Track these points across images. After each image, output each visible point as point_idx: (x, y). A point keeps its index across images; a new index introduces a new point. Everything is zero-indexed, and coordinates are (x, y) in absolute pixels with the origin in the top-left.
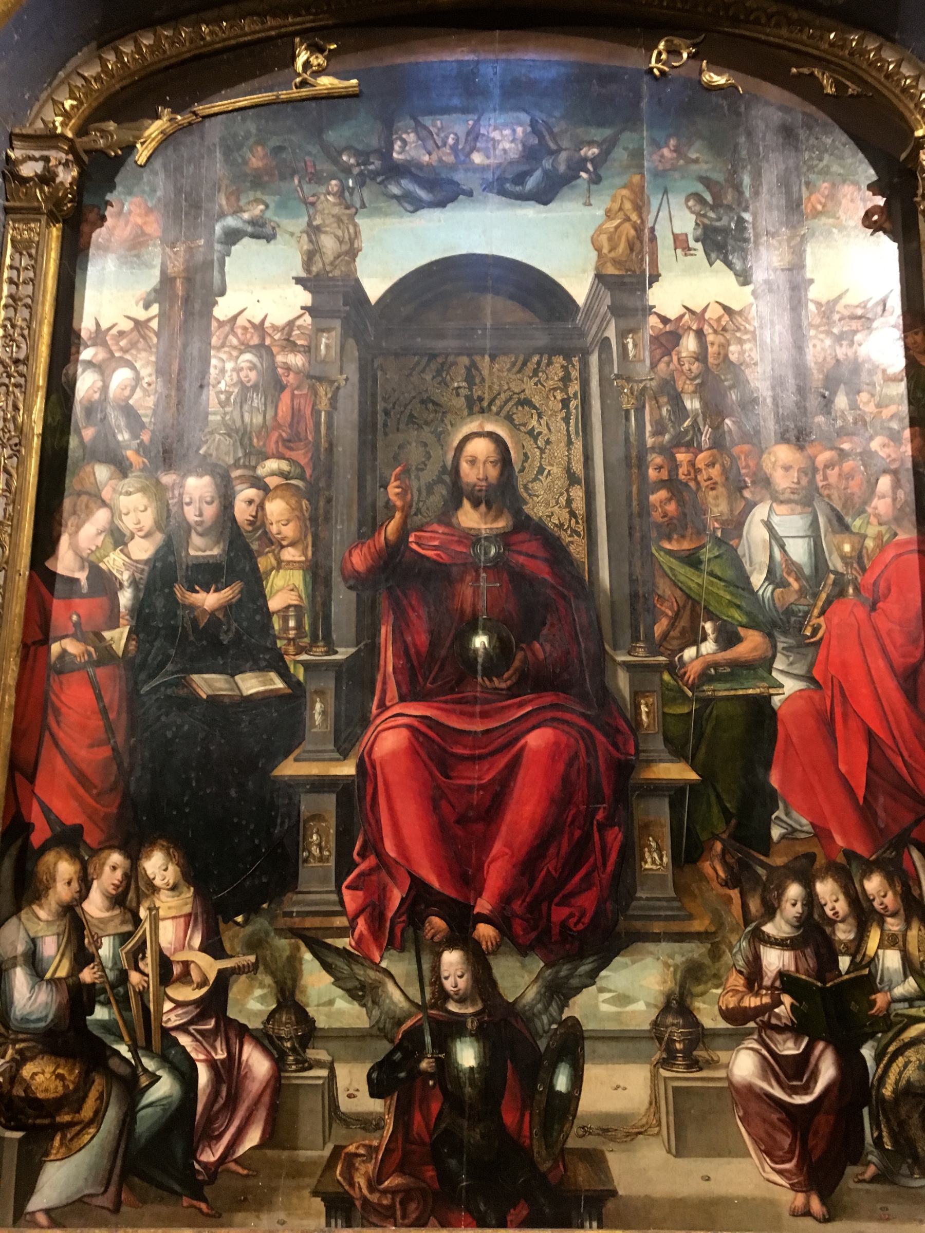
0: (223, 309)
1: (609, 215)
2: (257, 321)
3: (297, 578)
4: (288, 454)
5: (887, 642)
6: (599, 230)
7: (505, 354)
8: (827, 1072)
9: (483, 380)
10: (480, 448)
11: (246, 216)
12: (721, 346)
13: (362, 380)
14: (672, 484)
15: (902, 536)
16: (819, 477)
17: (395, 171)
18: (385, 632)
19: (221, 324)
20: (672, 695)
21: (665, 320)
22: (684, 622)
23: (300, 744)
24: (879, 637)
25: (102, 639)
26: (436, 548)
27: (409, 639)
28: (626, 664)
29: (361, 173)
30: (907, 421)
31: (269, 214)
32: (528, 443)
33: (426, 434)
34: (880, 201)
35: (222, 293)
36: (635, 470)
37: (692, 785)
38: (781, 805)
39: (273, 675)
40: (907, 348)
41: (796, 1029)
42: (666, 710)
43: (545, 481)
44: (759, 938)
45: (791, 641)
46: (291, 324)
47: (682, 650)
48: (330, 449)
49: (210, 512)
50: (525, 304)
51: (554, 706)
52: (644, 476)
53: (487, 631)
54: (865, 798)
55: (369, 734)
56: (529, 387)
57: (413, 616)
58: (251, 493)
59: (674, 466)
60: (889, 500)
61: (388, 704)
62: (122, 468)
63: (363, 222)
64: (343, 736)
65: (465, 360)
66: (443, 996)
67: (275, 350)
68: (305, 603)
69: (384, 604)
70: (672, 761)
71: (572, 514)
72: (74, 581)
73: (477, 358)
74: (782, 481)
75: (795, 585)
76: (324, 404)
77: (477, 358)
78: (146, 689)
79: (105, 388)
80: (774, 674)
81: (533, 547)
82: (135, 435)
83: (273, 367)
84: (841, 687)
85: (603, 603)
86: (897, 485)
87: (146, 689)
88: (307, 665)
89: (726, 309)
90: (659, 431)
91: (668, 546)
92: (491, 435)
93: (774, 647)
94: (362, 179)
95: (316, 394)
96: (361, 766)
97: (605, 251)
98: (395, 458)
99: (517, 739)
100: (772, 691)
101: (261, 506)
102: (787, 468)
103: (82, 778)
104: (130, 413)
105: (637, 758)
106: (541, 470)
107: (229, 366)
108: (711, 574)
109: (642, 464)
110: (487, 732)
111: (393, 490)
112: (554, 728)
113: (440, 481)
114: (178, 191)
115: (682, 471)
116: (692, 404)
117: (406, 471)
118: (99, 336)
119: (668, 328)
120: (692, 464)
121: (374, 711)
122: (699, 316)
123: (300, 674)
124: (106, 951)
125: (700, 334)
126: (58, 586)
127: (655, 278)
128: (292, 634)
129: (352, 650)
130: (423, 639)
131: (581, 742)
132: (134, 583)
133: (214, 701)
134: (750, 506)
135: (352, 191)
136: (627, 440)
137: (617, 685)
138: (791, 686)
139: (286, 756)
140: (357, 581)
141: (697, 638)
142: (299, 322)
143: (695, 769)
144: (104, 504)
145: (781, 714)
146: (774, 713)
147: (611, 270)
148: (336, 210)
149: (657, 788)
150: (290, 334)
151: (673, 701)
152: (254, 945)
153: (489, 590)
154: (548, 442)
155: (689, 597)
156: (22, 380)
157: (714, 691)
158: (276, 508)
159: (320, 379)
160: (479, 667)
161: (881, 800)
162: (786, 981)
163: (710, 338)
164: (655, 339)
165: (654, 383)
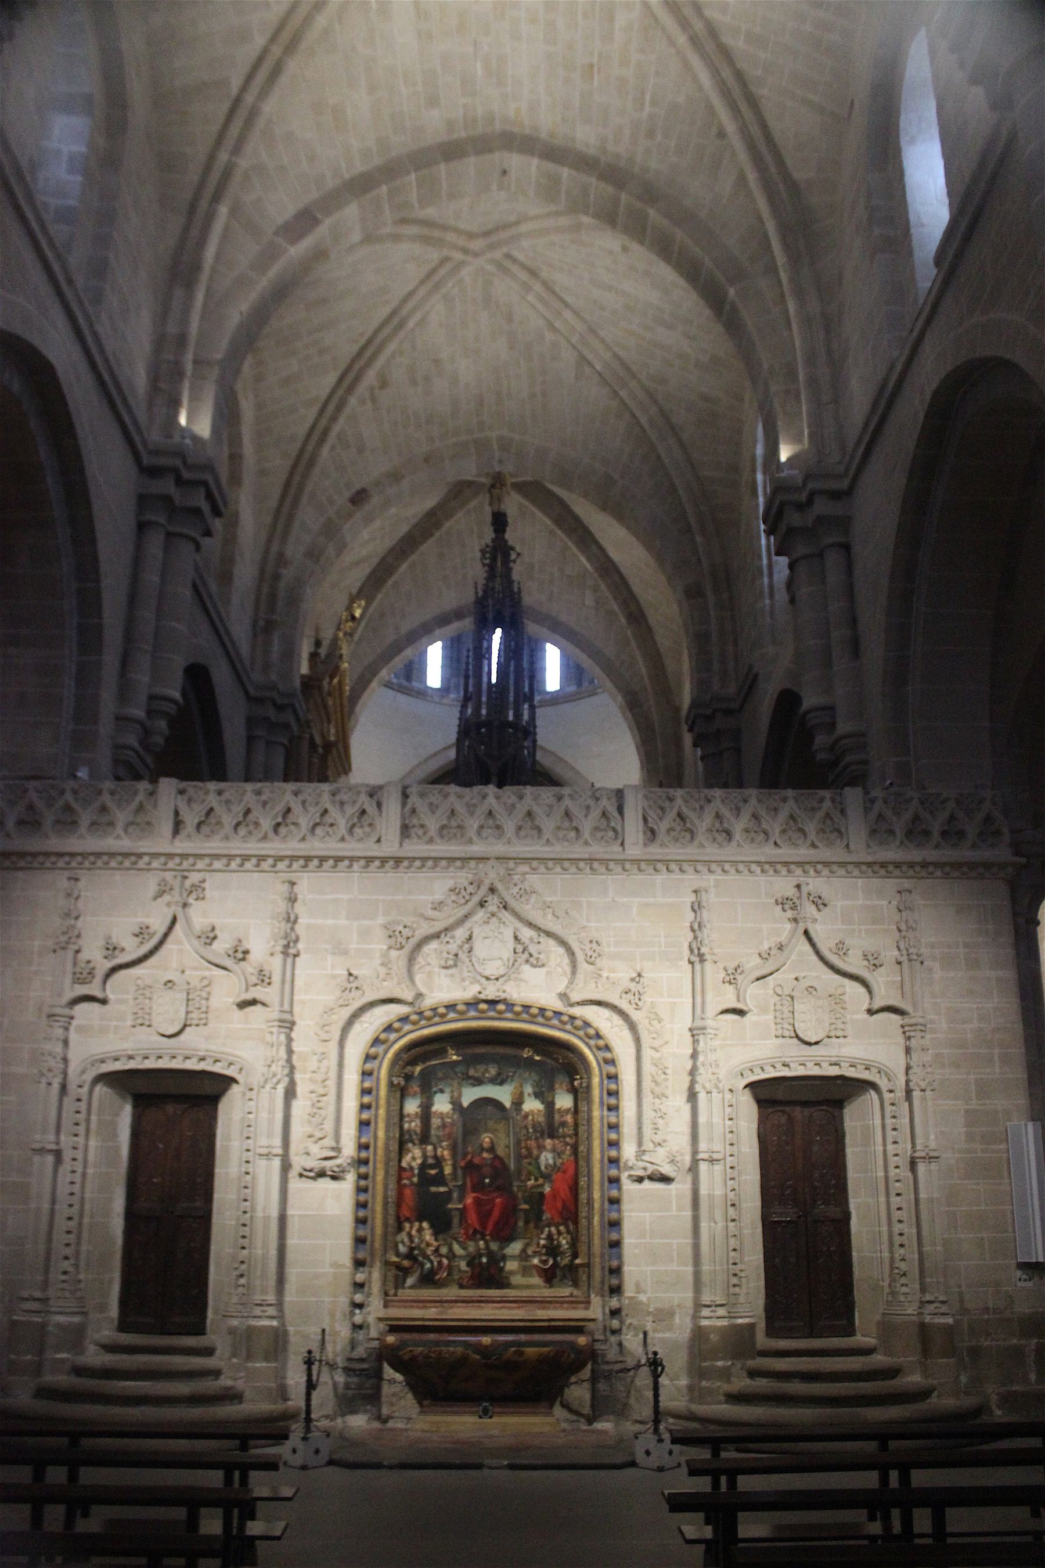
0: (434, 1109)
8: (551, 1262)
10: (487, 1140)
17: (470, 1077)
41: (546, 1254)
44: (540, 1238)
62: (414, 1144)
66: (479, 1249)
74: (549, 1147)
104: (415, 1131)
116: (531, 1130)
118: (409, 1115)
124: (416, 1240)
141: (530, 1180)
149: (522, 1210)
152: (444, 1240)
162: (544, 1246)
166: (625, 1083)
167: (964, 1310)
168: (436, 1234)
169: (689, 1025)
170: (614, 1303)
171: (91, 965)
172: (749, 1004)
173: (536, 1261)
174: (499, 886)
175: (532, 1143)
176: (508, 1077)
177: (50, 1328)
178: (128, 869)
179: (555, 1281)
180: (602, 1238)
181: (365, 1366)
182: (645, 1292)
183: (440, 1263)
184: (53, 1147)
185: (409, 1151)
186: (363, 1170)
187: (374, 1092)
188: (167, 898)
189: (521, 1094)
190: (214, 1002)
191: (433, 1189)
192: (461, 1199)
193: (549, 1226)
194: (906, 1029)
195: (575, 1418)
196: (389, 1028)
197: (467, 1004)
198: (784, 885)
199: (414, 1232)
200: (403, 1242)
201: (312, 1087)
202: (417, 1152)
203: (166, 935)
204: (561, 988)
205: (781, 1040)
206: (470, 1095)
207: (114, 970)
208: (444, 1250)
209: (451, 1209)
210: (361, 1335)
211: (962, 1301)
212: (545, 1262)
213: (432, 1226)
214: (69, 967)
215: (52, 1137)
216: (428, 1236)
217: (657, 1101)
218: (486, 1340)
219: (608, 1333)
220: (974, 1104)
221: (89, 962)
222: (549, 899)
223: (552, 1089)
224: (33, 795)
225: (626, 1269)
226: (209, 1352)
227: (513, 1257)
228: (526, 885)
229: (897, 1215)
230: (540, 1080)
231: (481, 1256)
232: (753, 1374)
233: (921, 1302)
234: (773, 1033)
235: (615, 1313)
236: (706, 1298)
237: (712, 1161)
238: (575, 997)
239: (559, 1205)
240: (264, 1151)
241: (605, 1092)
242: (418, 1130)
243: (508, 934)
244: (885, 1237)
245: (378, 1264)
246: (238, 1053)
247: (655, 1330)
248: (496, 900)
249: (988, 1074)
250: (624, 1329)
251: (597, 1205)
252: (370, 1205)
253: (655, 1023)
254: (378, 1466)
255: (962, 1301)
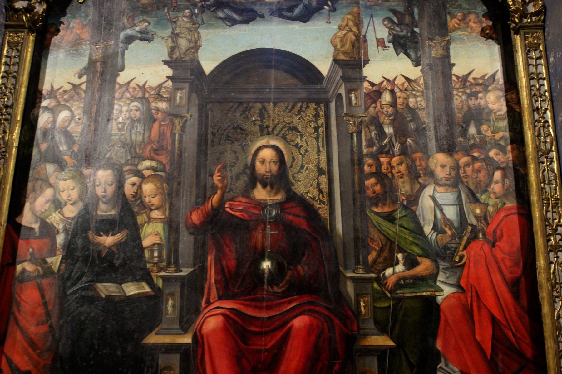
0: (122, 78)
1: (340, 28)
2: (141, 84)
3: (159, 228)
4: (156, 157)
5: (502, 265)
6: (335, 36)
7: (282, 102)
9: (269, 116)
10: (267, 154)
11: (137, 29)
12: (404, 98)
13: (200, 116)
14: (378, 175)
15: (509, 205)
16: (461, 171)
18: (211, 259)
19: (121, 86)
20: (379, 296)
21: (372, 84)
22: (385, 254)
23: (159, 324)
24: (497, 262)
25: (46, 262)
26: (240, 211)
27: (224, 263)
28: (351, 278)
29: (202, 6)
30: (509, 141)
31: (150, 28)
32: (295, 152)
33: (236, 146)
34: (490, 23)
35: (122, 69)
36: (357, 167)
37: (390, 348)
38: (443, 360)
39: (144, 284)
40: (507, 101)
42: (376, 305)
43: (305, 173)
45: (447, 264)
46: (160, 86)
47: (384, 270)
48: (180, 155)
49: (110, 190)
50: (294, 75)
51: (309, 303)
52: (362, 170)
53: (271, 259)
54: (491, 355)
55: (200, 319)
56: (296, 120)
57: (227, 250)
58: (134, 179)
59: (379, 165)
60: (500, 185)
61: (212, 301)
62: (61, 165)
63: (203, 31)
64: (185, 320)
65: (259, 105)
67: (151, 100)
68: (164, 242)
69: (210, 243)
70: (379, 335)
71: (320, 191)
72: (31, 229)
73: (266, 104)
74: (441, 173)
75: (449, 233)
76: (178, 129)
77: (266, 104)
78: (70, 291)
79: (54, 122)
80: (438, 283)
81: (298, 210)
82: (70, 148)
83: (149, 109)
84: (476, 291)
85: (338, 242)
86: (504, 176)
87: (70, 291)
88: (164, 278)
89: (407, 79)
90: (370, 144)
91: (376, 210)
92: (274, 147)
93: (438, 268)
94: (203, 10)
95: (173, 123)
96: (195, 338)
97: (339, 47)
98: (218, 159)
99: (288, 322)
100: (437, 293)
101: (140, 187)
102: (443, 166)
103: (32, 343)
104: (68, 135)
105: (359, 333)
106: (302, 167)
107: (125, 109)
108: (401, 226)
109: (361, 163)
110: (270, 318)
111: (216, 178)
112: (309, 315)
113: (244, 172)
114: (101, 16)
115: (384, 167)
116: (389, 130)
117: (224, 167)
118: (53, 93)
119: (374, 88)
120: (389, 163)
121: (203, 305)
122: (392, 82)
123: (160, 283)
125: (392, 92)
126: (23, 231)
127: (367, 61)
128: (156, 260)
129: (191, 270)
130: (233, 263)
131: (325, 324)
132: (66, 230)
133: (109, 299)
134: (423, 187)
135: (196, 16)
136: (352, 150)
137: (346, 290)
138: (448, 290)
139: (151, 331)
140: (194, 230)
141: (393, 263)
142: (166, 85)
143: (392, 339)
144: (50, 185)
145: (444, 307)
146: (438, 306)
147: (342, 57)
148: (188, 25)
150: (159, 91)
151: (380, 299)
153: (272, 235)
154: (306, 151)
155: (388, 239)
156: (9, 117)
157: (403, 293)
158: (148, 188)
159: (176, 116)
160: (266, 280)
161: (500, 356)
163: (398, 94)
164: (367, 95)
165: (366, 119)
209: (157, 347)
242: (76, 129)
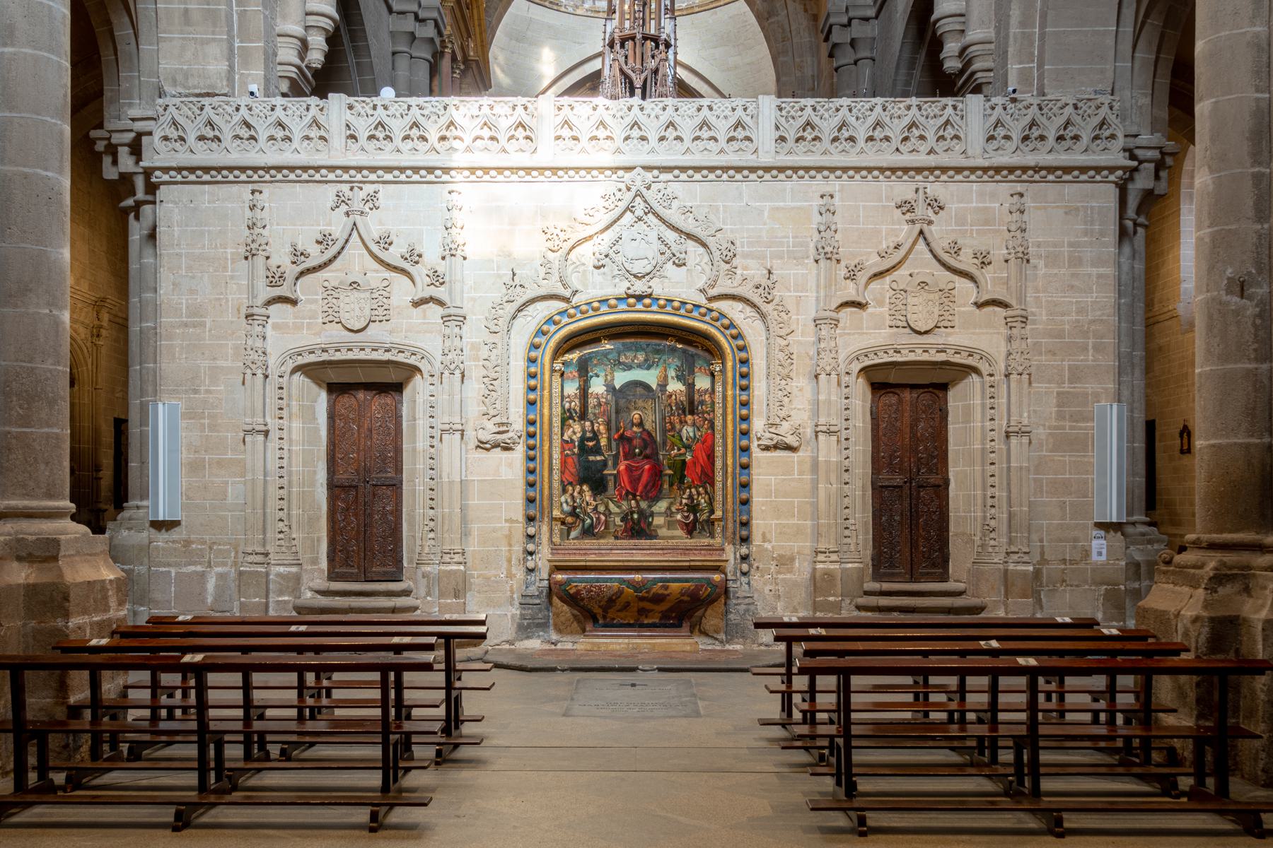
0: (590, 391)
8: (692, 517)
10: (637, 416)
14: (670, 422)
17: (620, 363)
74: (689, 422)
141: (673, 449)
158: (601, 427)
162: (686, 504)
166: (755, 367)
167: (1043, 561)
168: (594, 496)
169: (813, 315)
170: (744, 550)
171: (280, 270)
172: (867, 297)
173: (679, 517)
174: (644, 191)
175: (676, 419)
176: (654, 362)
177: (271, 577)
178: (307, 182)
179: (695, 533)
180: (734, 496)
181: (538, 601)
182: (770, 542)
183: (598, 519)
184: (263, 428)
185: (570, 426)
186: (531, 442)
187: (539, 376)
188: (344, 208)
189: (666, 377)
190: (394, 301)
191: (591, 458)
192: (615, 465)
193: (690, 488)
194: (1009, 320)
195: (711, 641)
196: (551, 320)
197: (617, 299)
198: (904, 189)
199: (575, 494)
200: (566, 502)
201: (485, 372)
202: (577, 427)
203: (347, 241)
204: (700, 285)
205: (895, 330)
206: (621, 378)
207: (302, 274)
208: (601, 509)
210: (532, 578)
211: (1042, 553)
212: (687, 517)
213: (592, 489)
214: (261, 272)
215: (261, 420)
216: (588, 496)
217: (783, 382)
218: (638, 577)
219: (738, 574)
220: (1066, 387)
221: (279, 267)
222: (690, 204)
223: (692, 372)
224: (208, 109)
225: (754, 522)
226: (406, 593)
227: (660, 514)
228: (669, 191)
229: (990, 481)
230: (682, 365)
231: (632, 513)
232: (859, 608)
233: (1007, 553)
234: (888, 323)
235: (745, 558)
236: (822, 547)
237: (829, 433)
238: (713, 292)
239: (699, 470)
240: (447, 427)
241: (738, 375)
242: (578, 409)
243: (653, 236)
244: (979, 501)
245: (546, 519)
246: (418, 344)
247: (779, 573)
248: (643, 205)
249: (1082, 361)
250: (752, 571)
251: (730, 470)
252: (538, 471)
253: (783, 314)
254: (553, 670)
255: (1042, 553)
